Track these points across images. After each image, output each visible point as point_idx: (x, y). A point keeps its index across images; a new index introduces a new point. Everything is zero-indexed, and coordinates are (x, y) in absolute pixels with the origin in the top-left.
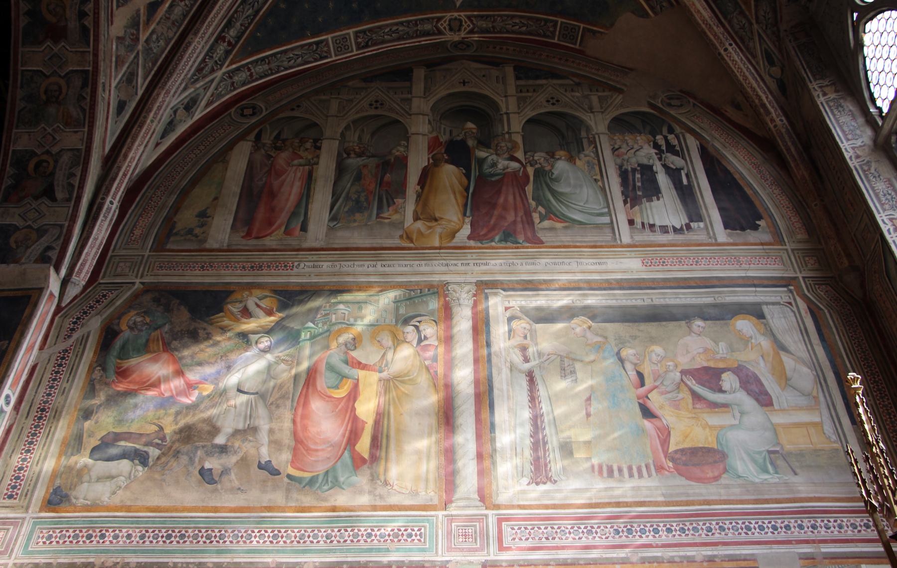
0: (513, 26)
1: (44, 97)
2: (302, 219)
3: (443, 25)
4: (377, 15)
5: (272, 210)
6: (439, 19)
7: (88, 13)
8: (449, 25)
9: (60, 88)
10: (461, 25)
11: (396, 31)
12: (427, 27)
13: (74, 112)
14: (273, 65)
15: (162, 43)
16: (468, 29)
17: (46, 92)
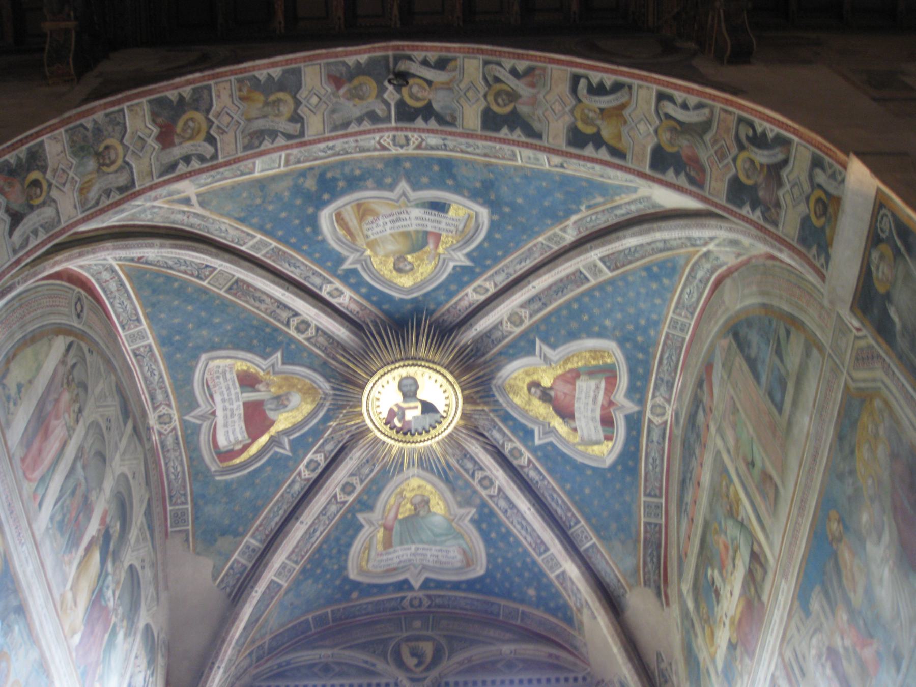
0: (173, 467)
1: (101, 149)
2: (43, 492)
3: (163, 410)
4: (168, 358)
5: (40, 451)
6: (169, 405)
7: (190, 166)
8: (164, 414)
9: (113, 163)
10: (165, 424)
11: (152, 374)
12: (160, 397)
13: (93, 194)
14: (117, 294)
15: (149, 217)
16: (163, 431)
17: (107, 148)
